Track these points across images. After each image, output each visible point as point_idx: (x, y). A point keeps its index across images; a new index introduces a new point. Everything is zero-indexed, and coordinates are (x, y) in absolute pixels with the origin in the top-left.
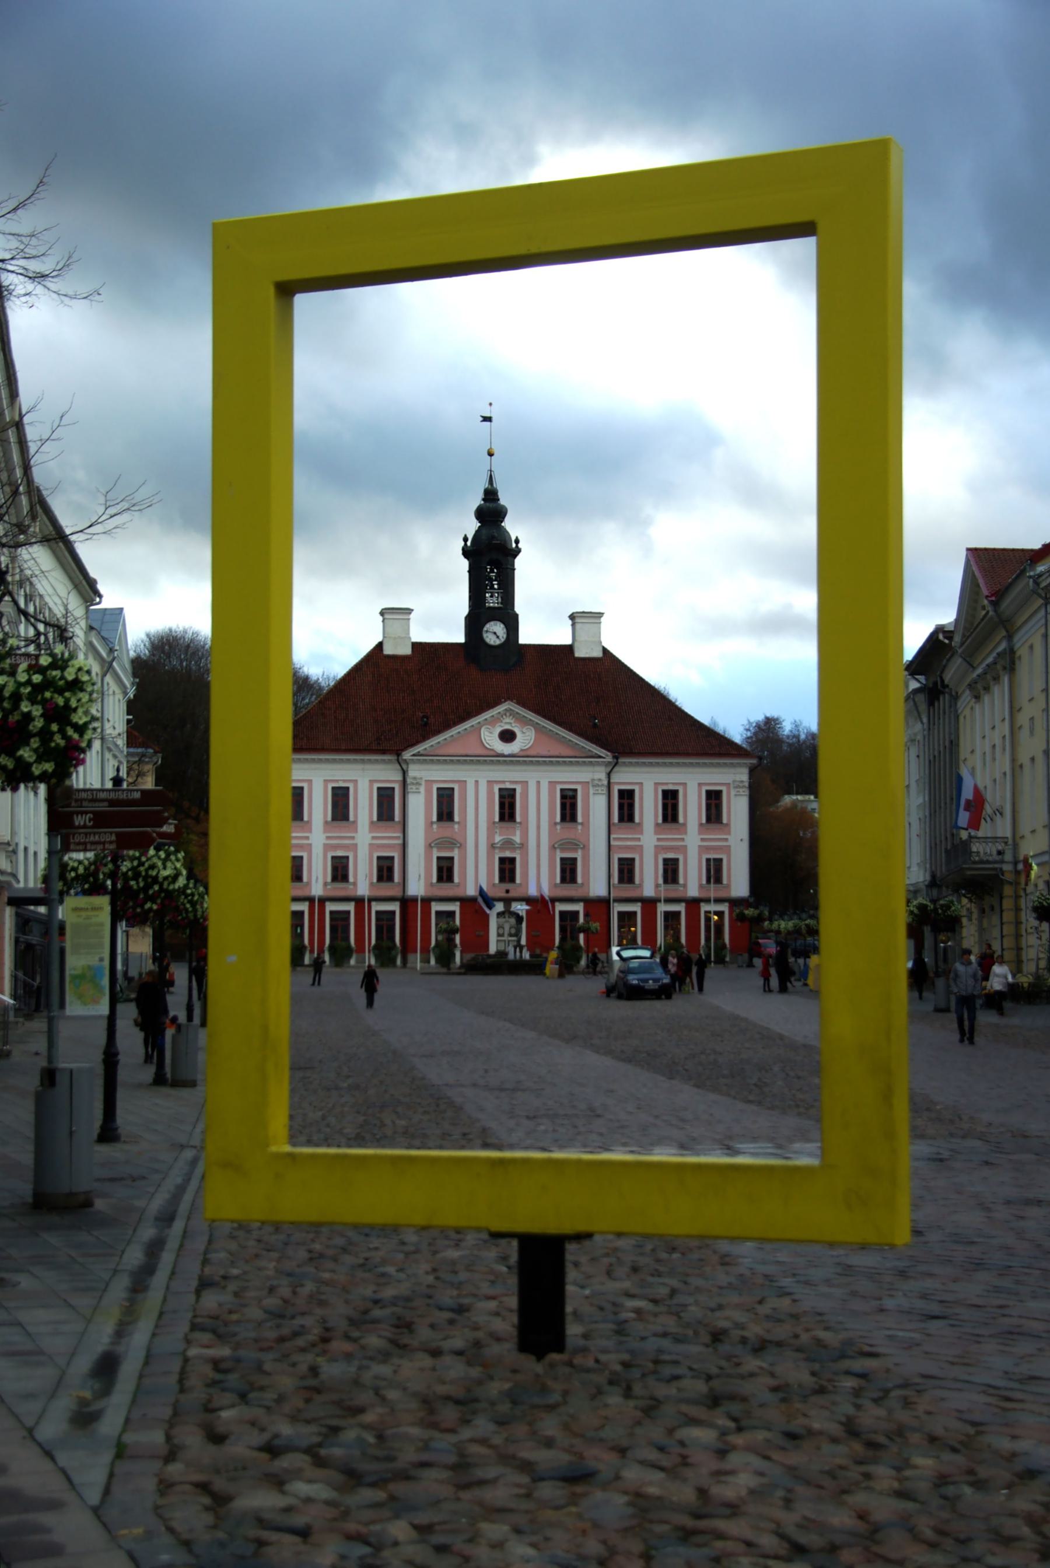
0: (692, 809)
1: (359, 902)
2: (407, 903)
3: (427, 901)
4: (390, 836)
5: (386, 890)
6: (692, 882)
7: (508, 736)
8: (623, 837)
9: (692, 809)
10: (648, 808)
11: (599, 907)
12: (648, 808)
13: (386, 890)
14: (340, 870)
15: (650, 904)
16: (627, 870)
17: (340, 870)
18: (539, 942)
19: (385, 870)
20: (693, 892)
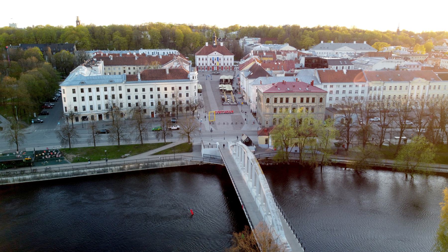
0: (229, 59)
1: (204, 67)
2: (208, 67)
3: (209, 66)
4: (206, 61)
5: (206, 65)
6: (229, 65)
7: (215, 54)
8: (224, 61)
9: (229, 59)
10: (226, 59)
11: (222, 67)
12: (226, 59)
13: (206, 65)
14: (203, 64)
15: (226, 66)
16: (224, 64)
17: (203, 64)
18: (218, 69)
19: (206, 64)
20: (229, 65)
